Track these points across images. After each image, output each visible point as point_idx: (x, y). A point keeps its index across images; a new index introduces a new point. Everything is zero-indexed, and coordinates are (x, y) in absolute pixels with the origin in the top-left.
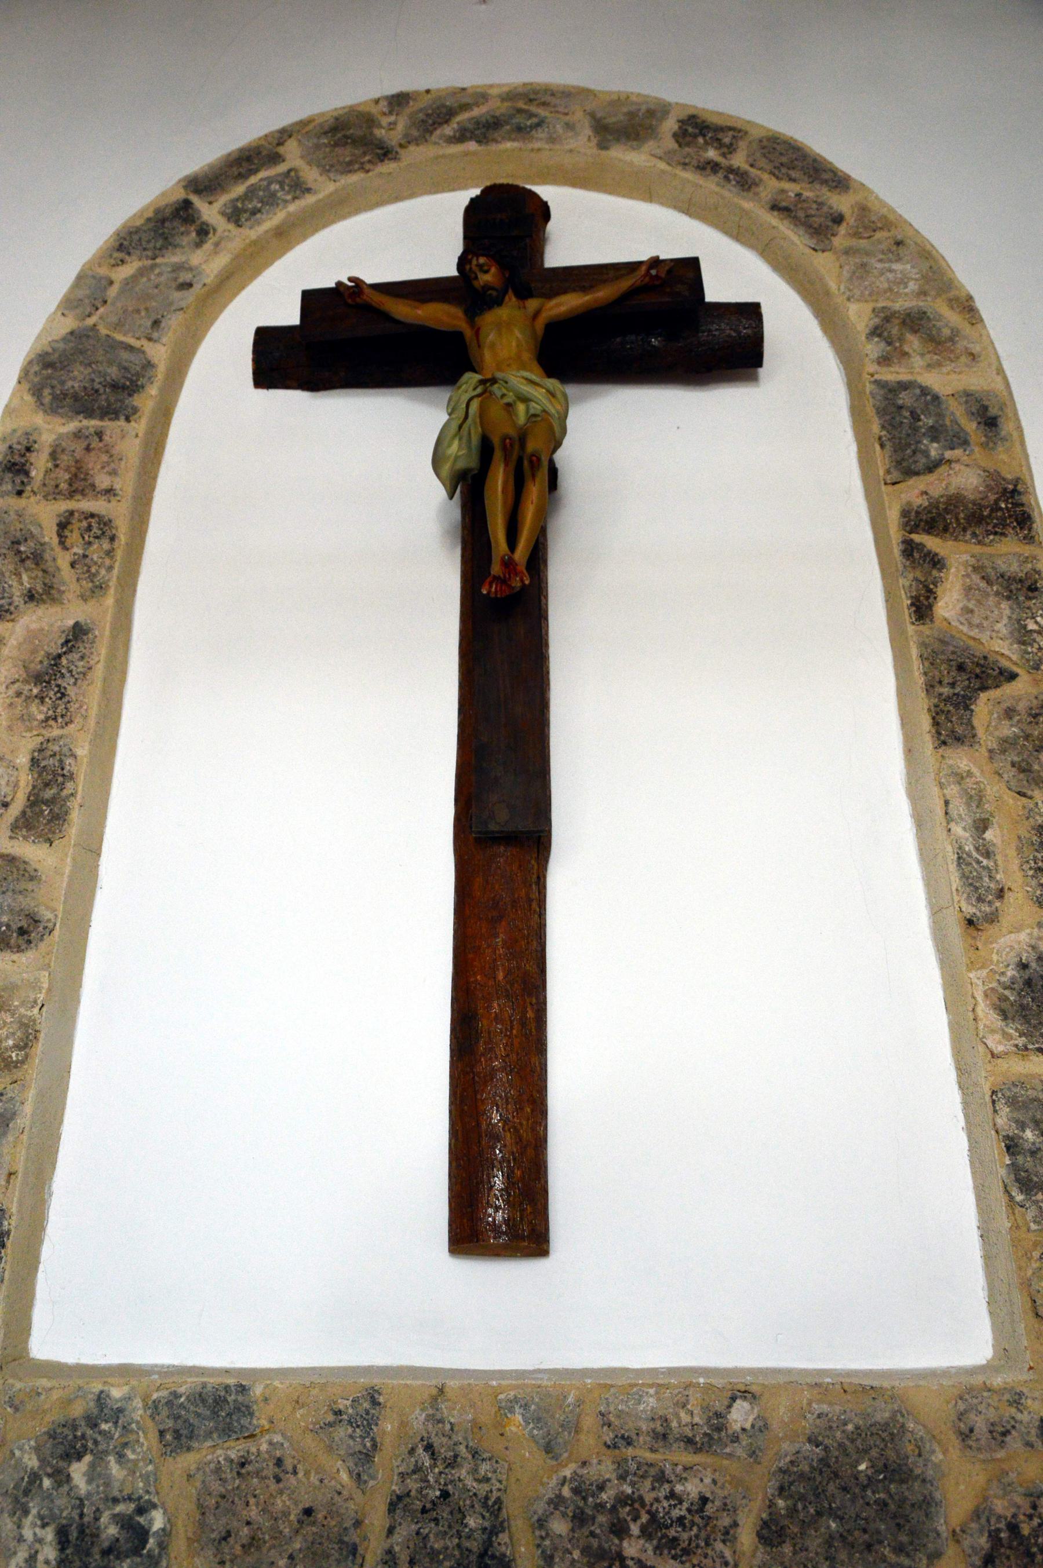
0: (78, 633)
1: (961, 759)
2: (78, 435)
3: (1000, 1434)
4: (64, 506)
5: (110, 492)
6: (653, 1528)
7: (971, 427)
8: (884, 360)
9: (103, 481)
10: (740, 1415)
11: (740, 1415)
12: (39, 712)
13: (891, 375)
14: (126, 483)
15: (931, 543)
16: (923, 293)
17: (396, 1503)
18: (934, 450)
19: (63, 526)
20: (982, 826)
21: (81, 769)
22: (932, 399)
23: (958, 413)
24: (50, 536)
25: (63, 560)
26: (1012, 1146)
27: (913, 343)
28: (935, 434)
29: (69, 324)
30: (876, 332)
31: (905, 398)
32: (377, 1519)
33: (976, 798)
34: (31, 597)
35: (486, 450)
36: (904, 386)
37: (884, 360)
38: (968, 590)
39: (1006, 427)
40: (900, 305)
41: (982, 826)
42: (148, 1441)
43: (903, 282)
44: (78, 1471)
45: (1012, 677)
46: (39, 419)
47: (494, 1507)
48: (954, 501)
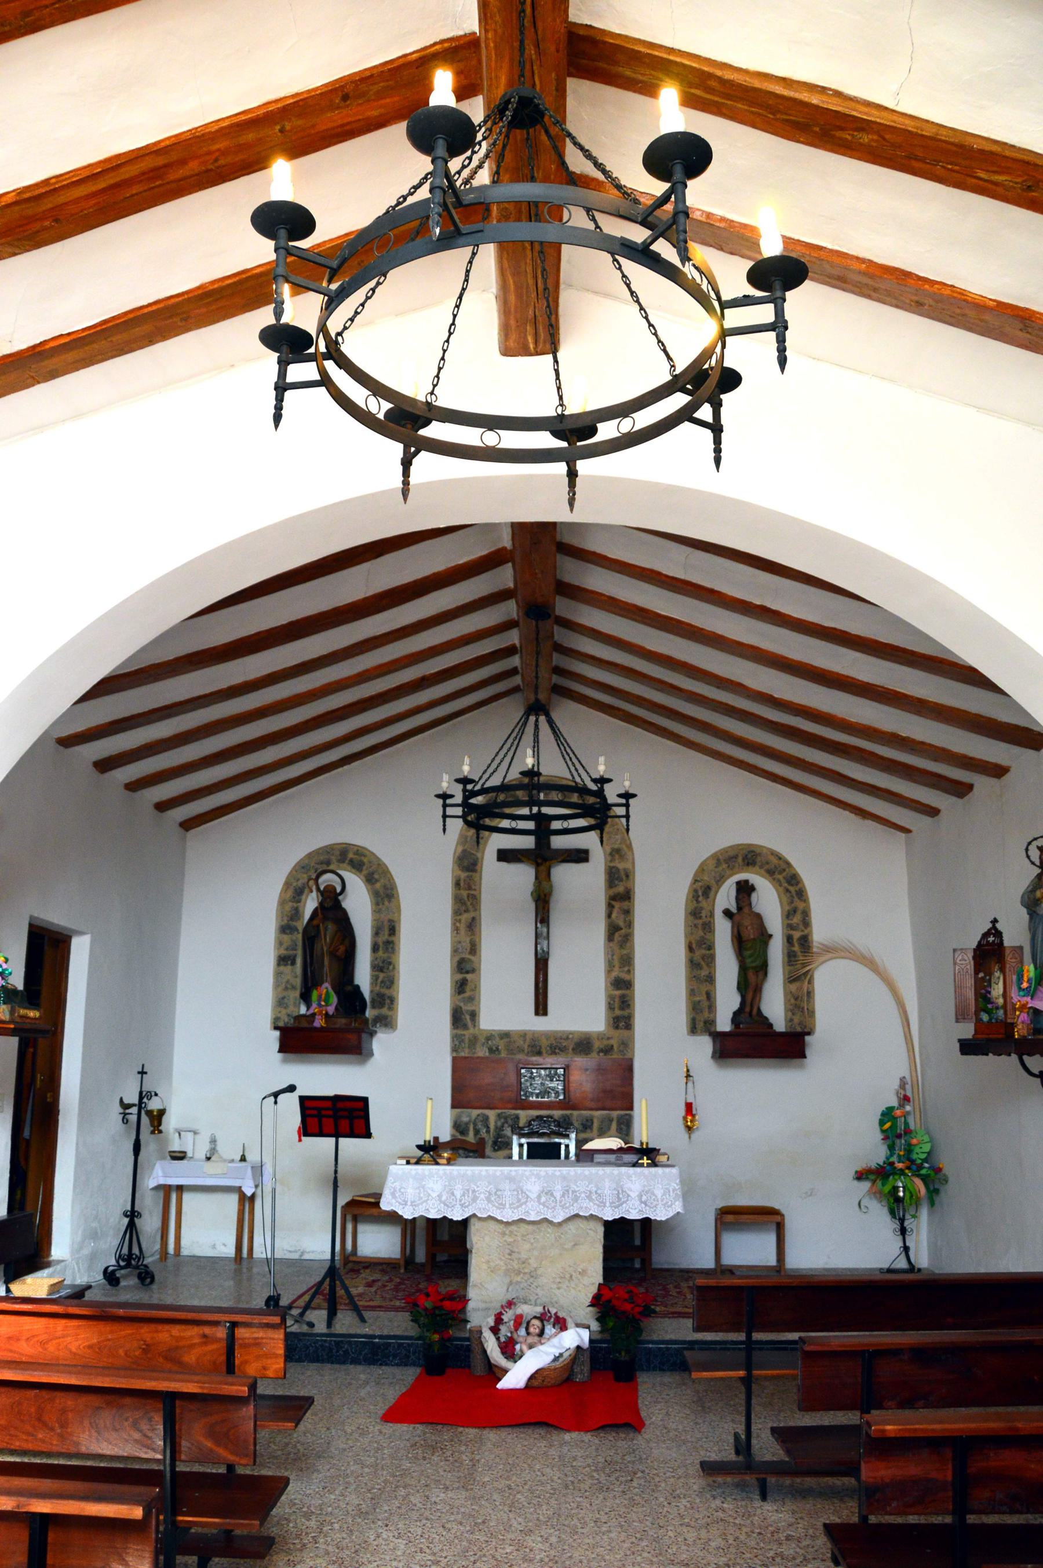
0: (473, 919)
1: (611, 944)
2: (468, 877)
3: (602, 1039)
4: (467, 892)
5: (475, 890)
6: (559, 1049)
7: (624, 878)
8: (611, 861)
9: (473, 887)
10: (571, 1036)
11: (571, 1036)
12: (470, 933)
13: (612, 865)
14: (477, 887)
15: (613, 903)
16: (620, 843)
17: (529, 1046)
18: (616, 882)
19: (468, 897)
20: (613, 955)
21: (477, 943)
22: (618, 870)
23: (622, 873)
24: (466, 898)
25: (469, 903)
26: (609, 1003)
27: (617, 856)
28: (617, 879)
29: (460, 849)
30: (611, 854)
31: (614, 870)
32: (526, 1047)
33: (612, 951)
34: (465, 911)
35: (539, 896)
36: (614, 867)
37: (611, 861)
38: (618, 913)
39: (631, 877)
40: (616, 846)
41: (613, 955)
42: (498, 1039)
43: (617, 840)
44: (490, 1042)
45: (622, 929)
46: (460, 872)
47: (541, 1047)
48: (619, 894)
